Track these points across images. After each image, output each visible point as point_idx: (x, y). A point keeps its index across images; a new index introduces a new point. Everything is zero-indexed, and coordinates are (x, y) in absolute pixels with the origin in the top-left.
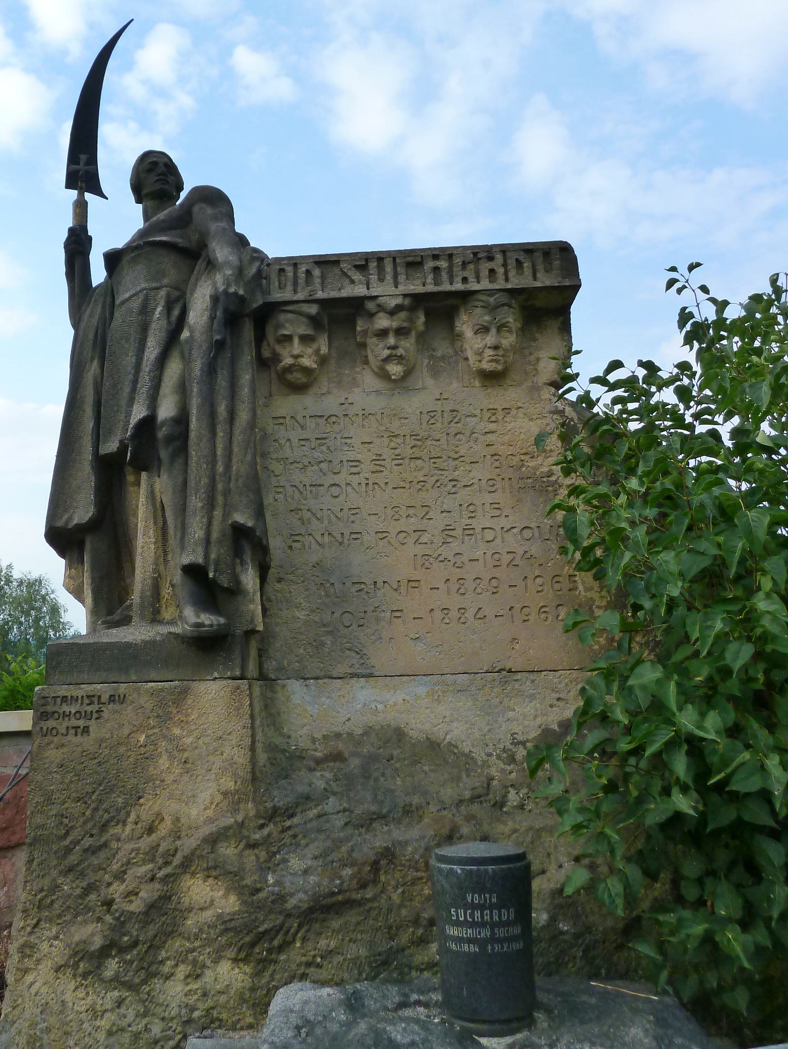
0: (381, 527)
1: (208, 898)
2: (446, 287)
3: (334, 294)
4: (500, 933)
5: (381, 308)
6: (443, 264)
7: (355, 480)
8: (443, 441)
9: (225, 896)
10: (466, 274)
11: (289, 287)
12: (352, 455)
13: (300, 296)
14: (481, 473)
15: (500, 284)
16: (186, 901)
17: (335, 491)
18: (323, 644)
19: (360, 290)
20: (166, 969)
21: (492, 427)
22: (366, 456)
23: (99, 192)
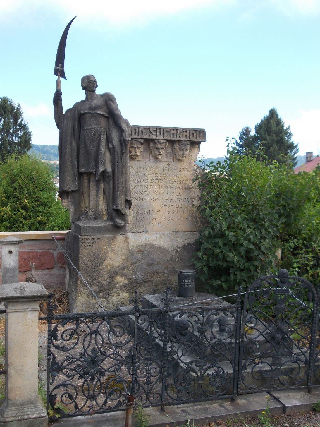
0: (152, 196)
1: (120, 280)
2: (175, 139)
3: (148, 138)
4: (191, 284)
5: (159, 142)
6: (175, 132)
7: (146, 184)
8: (168, 176)
9: (124, 280)
10: (180, 135)
11: (137, 134)
12: (145, 178)
13: (139, 137)
14: (176, 185)
15: (188, 139)
16: (116, 281)
17: (141, 187)
18: (136, 224)
19: (154, 137)
20: (112, 295)
21: (179, 173)
22: (149, 178)
23: (64, 77)
